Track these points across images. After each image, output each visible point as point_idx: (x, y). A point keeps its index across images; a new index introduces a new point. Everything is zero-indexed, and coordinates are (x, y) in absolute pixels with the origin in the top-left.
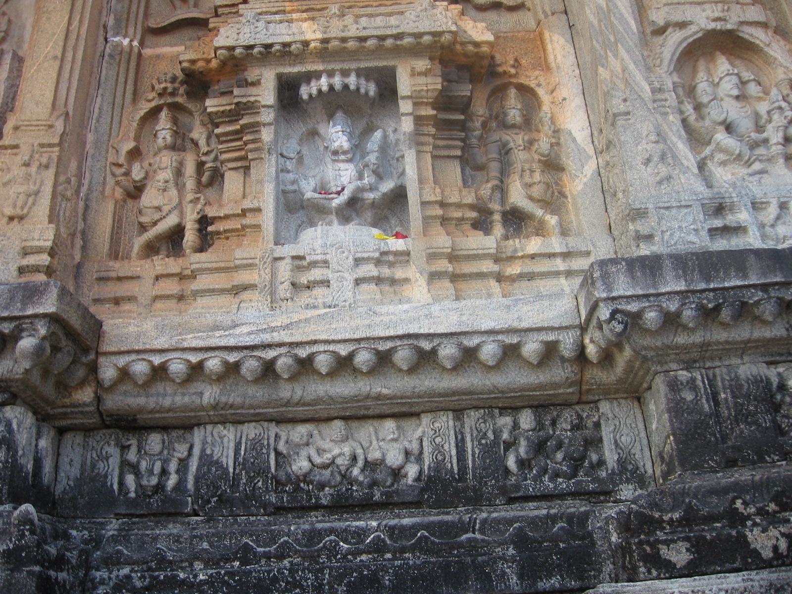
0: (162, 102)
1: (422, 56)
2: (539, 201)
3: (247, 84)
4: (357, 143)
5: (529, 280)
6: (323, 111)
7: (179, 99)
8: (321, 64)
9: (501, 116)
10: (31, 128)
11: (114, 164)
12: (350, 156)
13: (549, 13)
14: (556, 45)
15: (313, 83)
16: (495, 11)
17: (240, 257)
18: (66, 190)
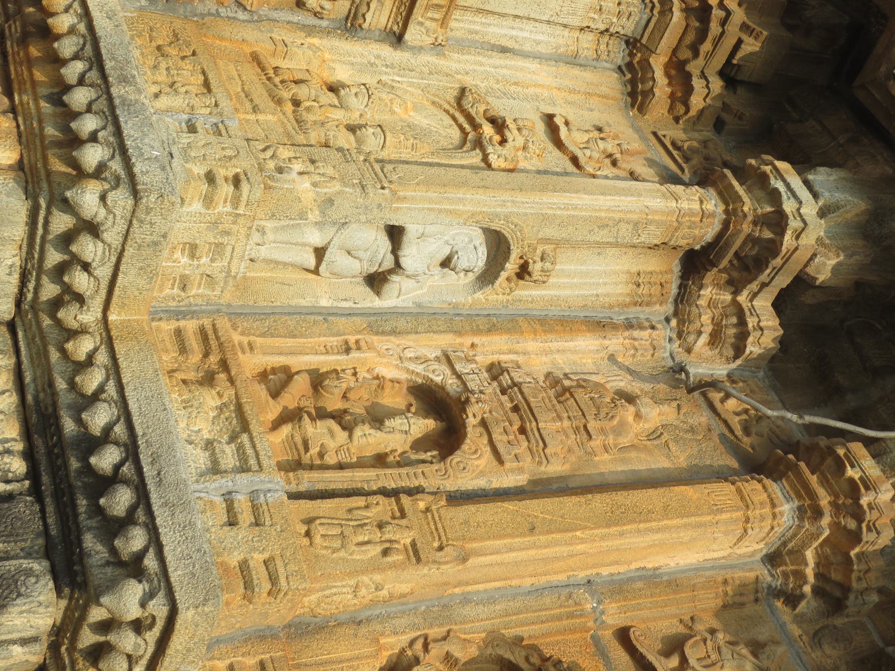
10: (432, 524)
11: (426, 639)
18: (367, 587)
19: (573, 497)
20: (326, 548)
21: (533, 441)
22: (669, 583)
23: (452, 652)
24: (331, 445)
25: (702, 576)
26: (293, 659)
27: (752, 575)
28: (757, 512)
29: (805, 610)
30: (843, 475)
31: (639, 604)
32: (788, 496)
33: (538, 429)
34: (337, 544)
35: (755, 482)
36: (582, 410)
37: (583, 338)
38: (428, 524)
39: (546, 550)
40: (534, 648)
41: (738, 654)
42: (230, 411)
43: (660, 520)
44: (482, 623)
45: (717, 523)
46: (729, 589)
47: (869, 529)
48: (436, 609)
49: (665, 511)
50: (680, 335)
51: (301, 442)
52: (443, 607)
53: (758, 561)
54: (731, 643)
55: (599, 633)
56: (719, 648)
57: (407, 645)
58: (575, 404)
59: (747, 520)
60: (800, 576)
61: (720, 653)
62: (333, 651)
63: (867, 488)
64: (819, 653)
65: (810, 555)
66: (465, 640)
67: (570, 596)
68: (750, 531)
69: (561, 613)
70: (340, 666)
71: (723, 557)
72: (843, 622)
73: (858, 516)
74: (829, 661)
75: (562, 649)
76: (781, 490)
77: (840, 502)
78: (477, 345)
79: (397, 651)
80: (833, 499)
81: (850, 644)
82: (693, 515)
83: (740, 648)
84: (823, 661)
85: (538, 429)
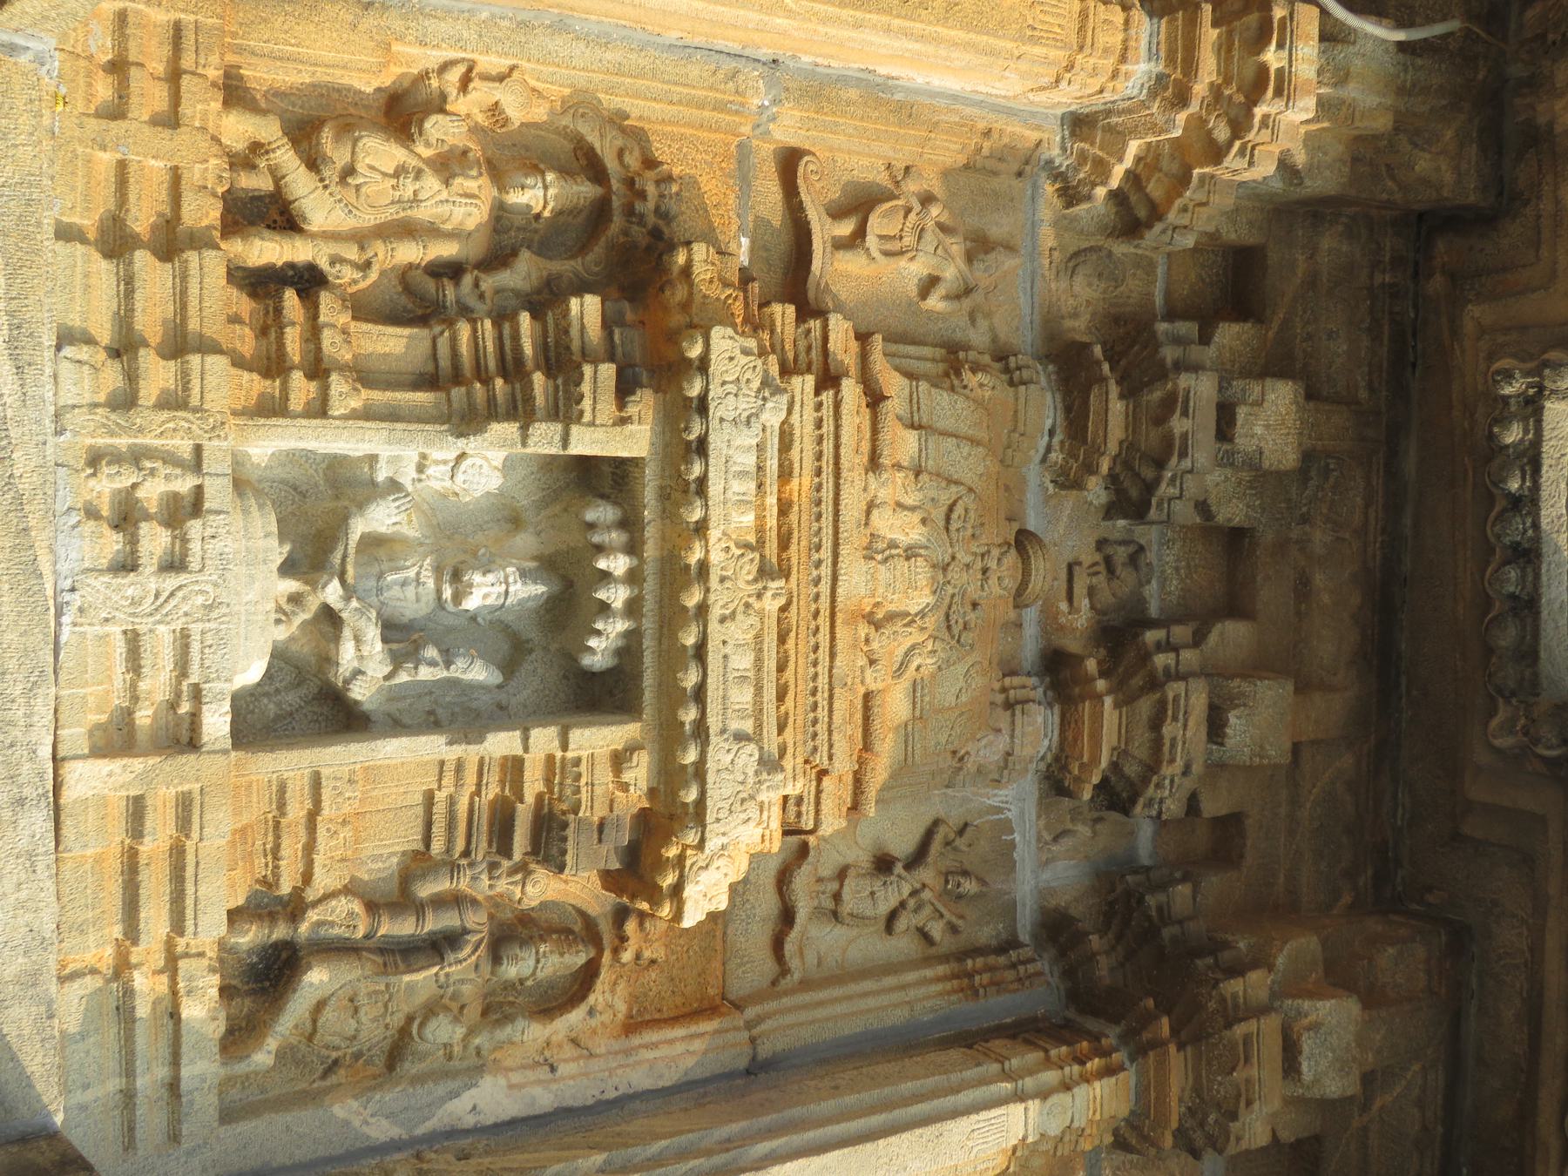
0: (615, 185)
1: (659, 773)
2: (314, 1021)
3: (624, 390)
4: (480, 620)
5: (118, 1008)
6: (564, 547)
7: (617, 222)
8: (657, 554)
9: (524, 933)
11: (470, 70)
12: (450, 607)
13: (755, 1032)
14: (680, 1048)
15: (616, 537)
16: (776, 912)
17: (207, 367)
22: (901, 106)
23: (504, 106)
25: (957, 112)
26: (234, 35)
27: (1034, 136)
28: (1092, 61)
29: (1083, 214)
30: (1258, 54)
31: (836, 124)
32: (1154, 50)
35: (1118, 8)
39: (723, 9)
40: (638, 136)
41: (946, 251)
43: (930, 23)
44: (573, 72)
45: (1019, 57)
46: (987, 145)
47: (1242, 152)
48: (506, 23)
49: (947, 11)
52: (518, 24)
53: (1055, 117)
54: (942, 227)
55: (755, 142)
56: (922, 229)
57: (436, 67)
59: (1070, 67)
60: (1101, 169)
61: (920, 238)
62: (308, 43)
63: (1278, 92)
64: (1064, 284)
65: (1134, 147)
66: (534, 90)
67: (734, 75)
68: (1064, 84)
69: (706, 97)
70: (312, 69)
71: (1005, 97)
72: (1125, 251)
73: (1239, 127)
74: (1071, 301)
75: (685, 150)
76: (1151, 35)
77: (1227, 92)
79: (416, 72)
80: (1220, 81)
81: (1116, 288)
82: (987, 34)
83: (953, 240)
84: (1063, 298)
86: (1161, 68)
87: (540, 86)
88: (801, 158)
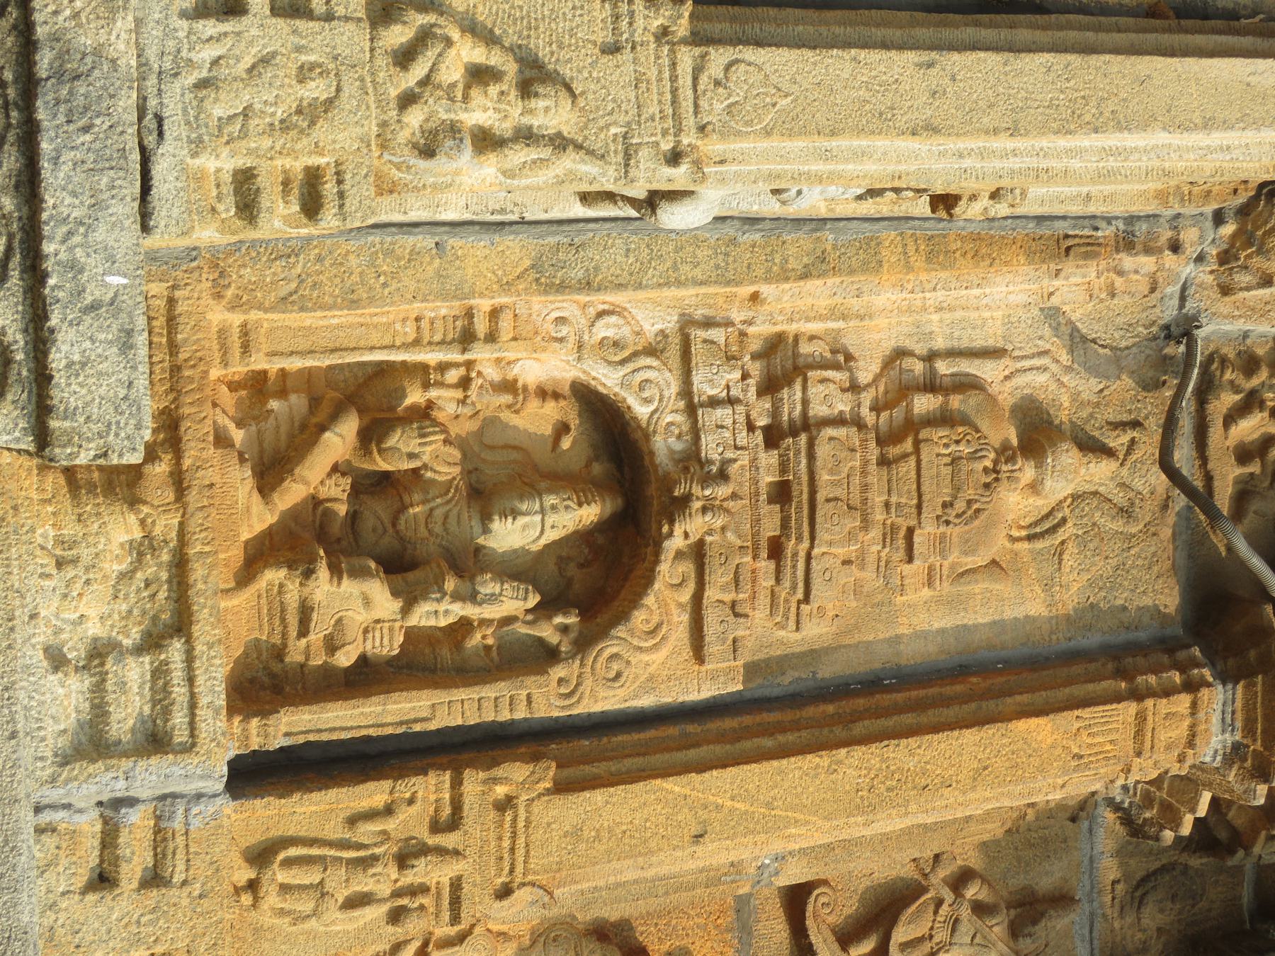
19: (809, 757)
20: (282, 913)
21: (787, 584)
24: (358, 617)
32: (1229, 720)
33: (809, 557)
34: (306, 906)
36: (920, 496)
37: (1009, 277)
38: (500, 839)
41: (985, 938)
42: (159, 565)
49: (975, 779)
50: (1225, 258)
51: (296, 605)
56: (957, 920)
58: (913, 474)
61: (953, 930)
74: (1139, 935)
78: (763, 302)
85: (809, 557)
86: (1238, 737)
87: (504, 928)
88: (810, 893)
